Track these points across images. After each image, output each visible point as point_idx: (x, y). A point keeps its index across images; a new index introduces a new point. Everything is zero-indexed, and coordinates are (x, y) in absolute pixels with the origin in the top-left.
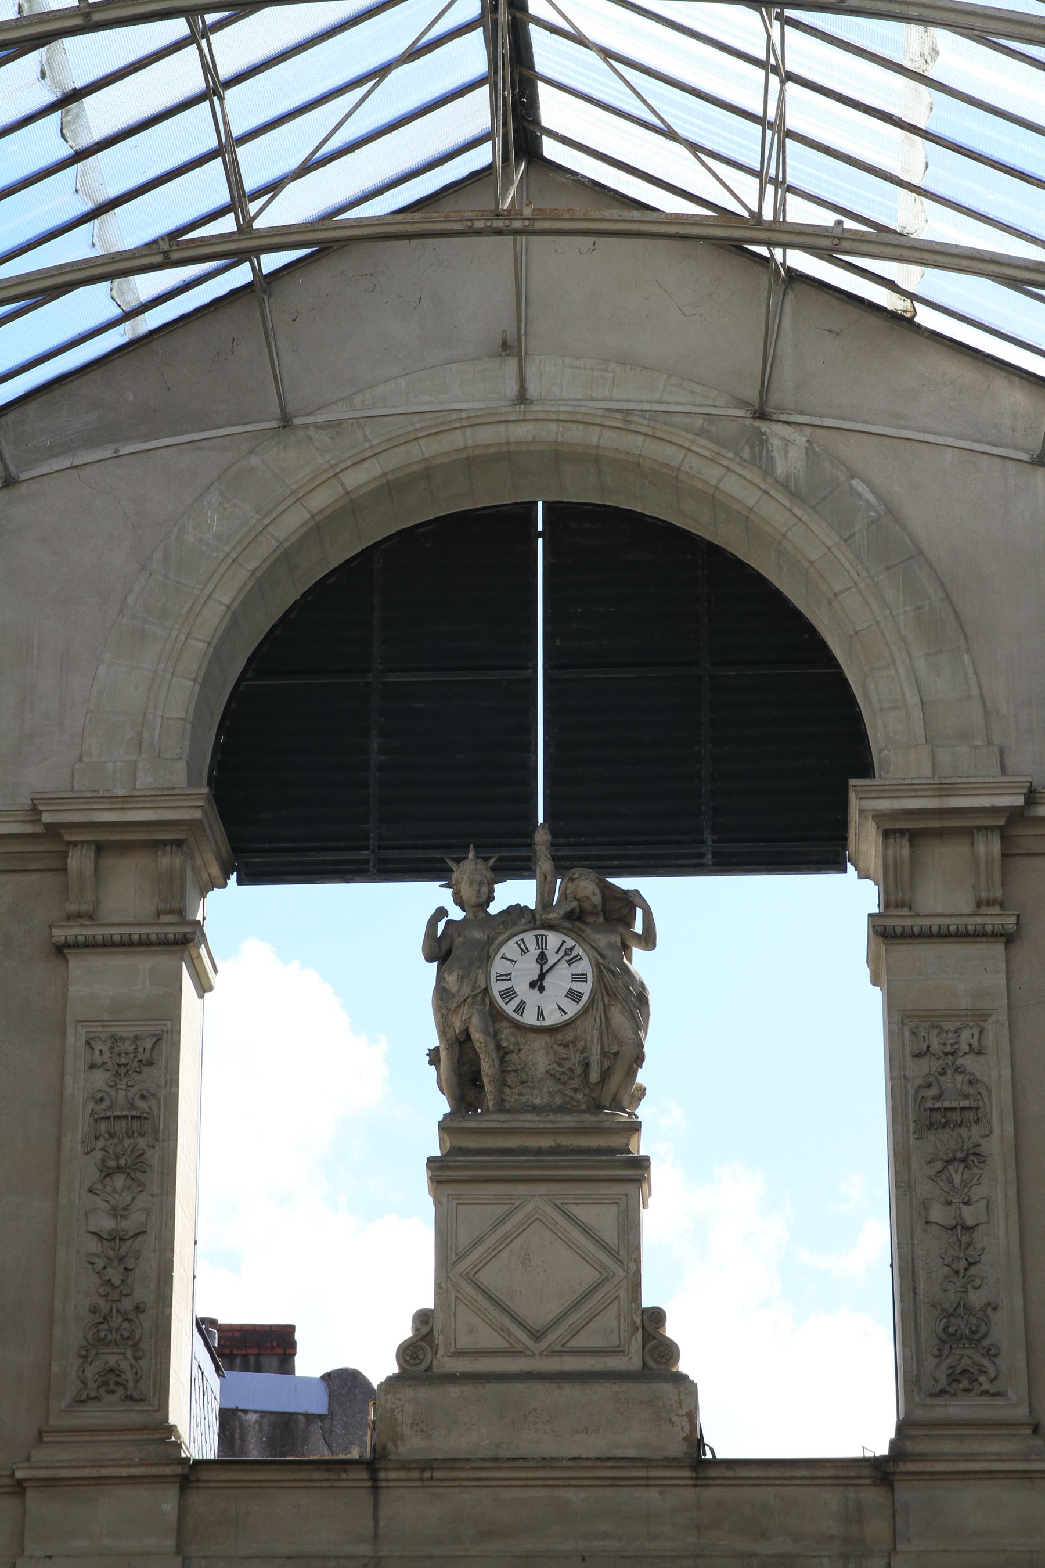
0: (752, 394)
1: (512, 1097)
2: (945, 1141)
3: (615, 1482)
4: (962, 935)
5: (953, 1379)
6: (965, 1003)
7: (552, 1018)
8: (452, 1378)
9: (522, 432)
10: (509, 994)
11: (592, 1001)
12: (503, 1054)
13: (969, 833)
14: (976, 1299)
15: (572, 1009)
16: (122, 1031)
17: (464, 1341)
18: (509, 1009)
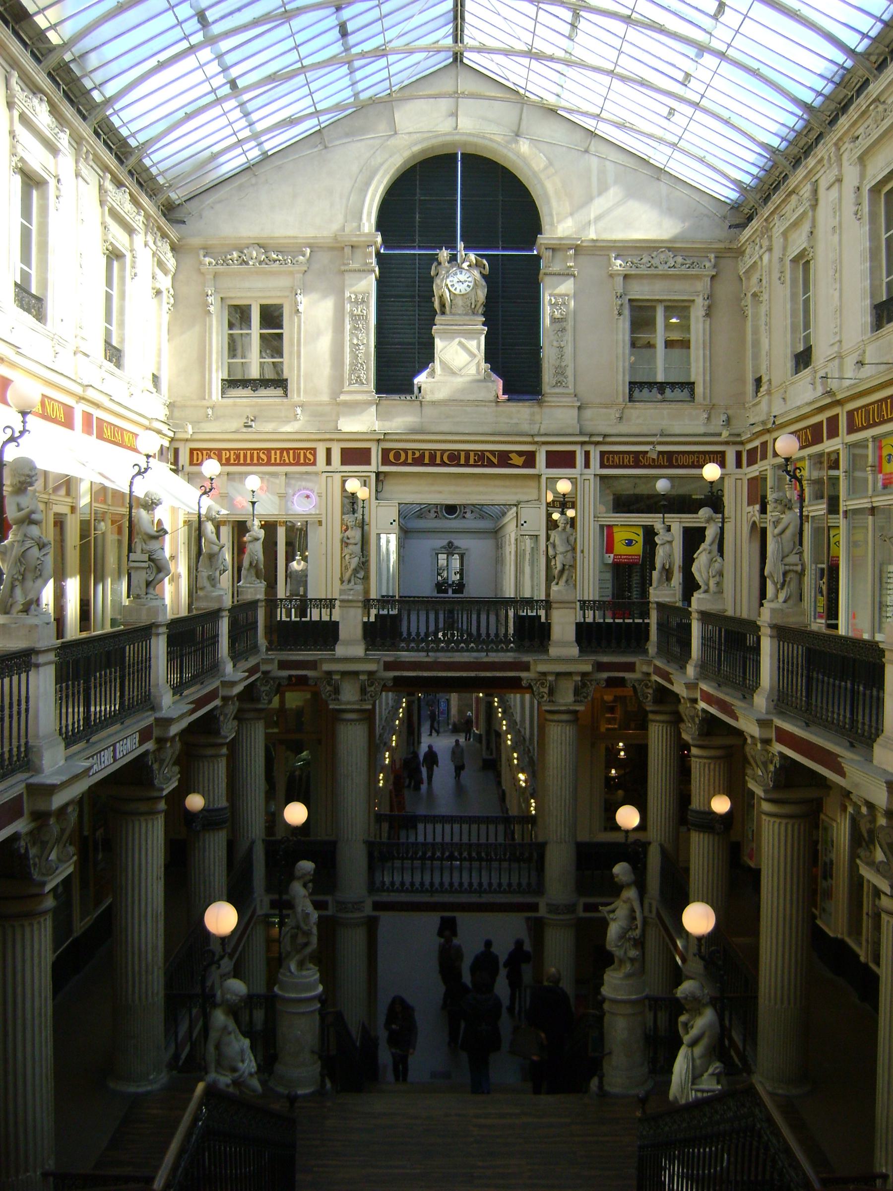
0: (515, 129)
1: (453, 311)
2: (557, 326)
3: (477, 406)
7: (463, 292)
9: (457, 138)
10: (452, 286)
15: (468, 289)
18: (452, 289)
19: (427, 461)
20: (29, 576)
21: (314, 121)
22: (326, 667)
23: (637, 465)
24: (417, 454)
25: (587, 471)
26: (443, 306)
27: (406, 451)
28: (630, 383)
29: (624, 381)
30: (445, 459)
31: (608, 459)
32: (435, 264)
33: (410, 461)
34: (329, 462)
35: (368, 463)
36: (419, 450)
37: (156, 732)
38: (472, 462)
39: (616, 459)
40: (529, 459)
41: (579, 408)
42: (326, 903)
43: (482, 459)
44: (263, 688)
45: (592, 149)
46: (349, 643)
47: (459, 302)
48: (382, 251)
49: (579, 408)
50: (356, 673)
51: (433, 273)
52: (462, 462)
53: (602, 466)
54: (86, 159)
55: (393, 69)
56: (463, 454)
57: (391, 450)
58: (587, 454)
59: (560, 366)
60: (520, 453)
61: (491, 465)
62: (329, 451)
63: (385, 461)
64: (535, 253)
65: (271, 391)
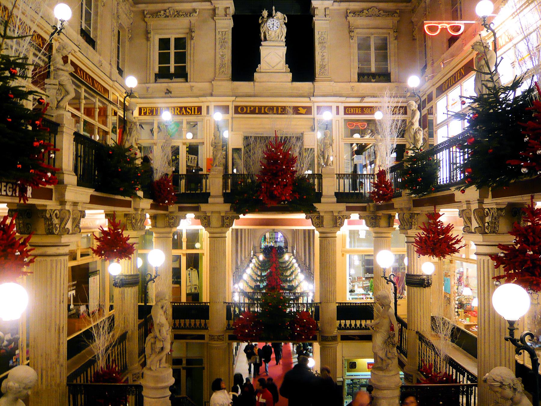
10: (269, 27)
19: (257, 111)
23: (363, 113)
24: (252, 108)
27: (246, 107)
31: (348, 111)
32: (261, 17)
33: (248, 112)
36: (253, 106)
38: (280, 112)
39: (352, 110)
42: (204, 336)
51: (260, 22)
53: (345, 114)
57: (239, 106)
60: (304, 107)
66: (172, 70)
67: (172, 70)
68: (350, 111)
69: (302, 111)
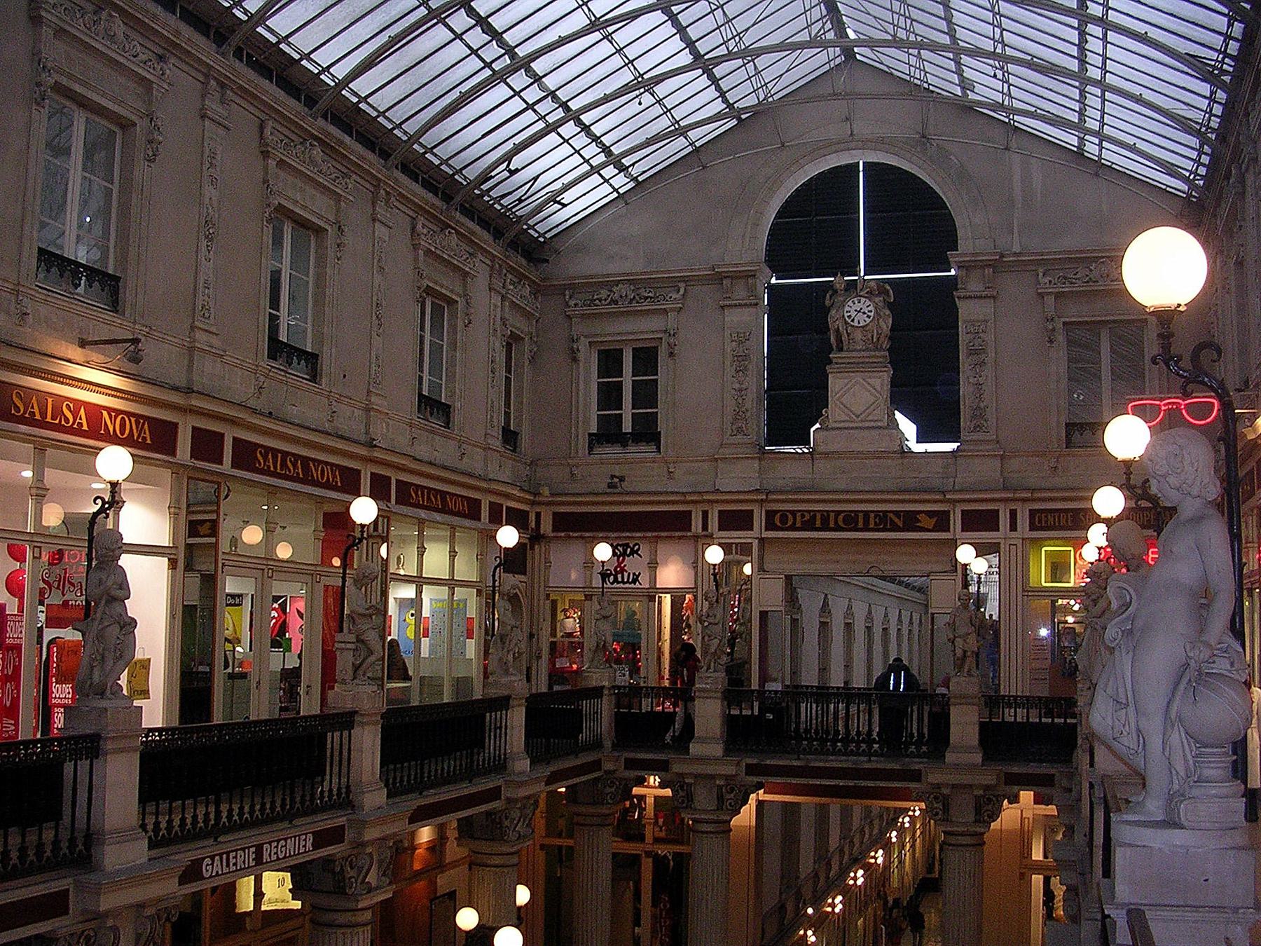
4: (981, 297)
5: (975, 428)
6: (981, 317)
8: (834, 429)
11: (874, 317)
12: (849, 335)
13: (983, 267)
14: (982, 405)
15: (868, 320)
16: (739, 330)
17: (838, 418)
19: (818, 524)
20: (110, 657)
21: (681, 141)
22: (676, 768)
24: (807, 517)
25: (1013, 534)
26: (839, 341)
27: (793, 513)
28: (1067, 425)
29: (1058, 422)
30: (841, 523)
32: (830, 292)
34: (705, 527)
35: (750, 527)
37: (349, 835)
40: (942, 521)
41: (1002, 457)
43: (884, 521)
44: (608, 790)
45: (1013, 145)
46: (703, 740)
47: (858, 335)
48: (773, 281)
49: (1002, 457)
50: (712, 777)
51: (827, 303)
52: (861, 525)
54: (387, 201)
55: (767, 76)
56: (861, 515)
57: (776, 512)
58: (1013, 514)
59: (978, 407)
61: (895, 528)
62: (705, 514)
63: (770, 526)
64: (953, 272)
65: (643, 448)
66: (627, 427)
67: (627, 427)
68: (1046, 522)
69: (926, 522)
